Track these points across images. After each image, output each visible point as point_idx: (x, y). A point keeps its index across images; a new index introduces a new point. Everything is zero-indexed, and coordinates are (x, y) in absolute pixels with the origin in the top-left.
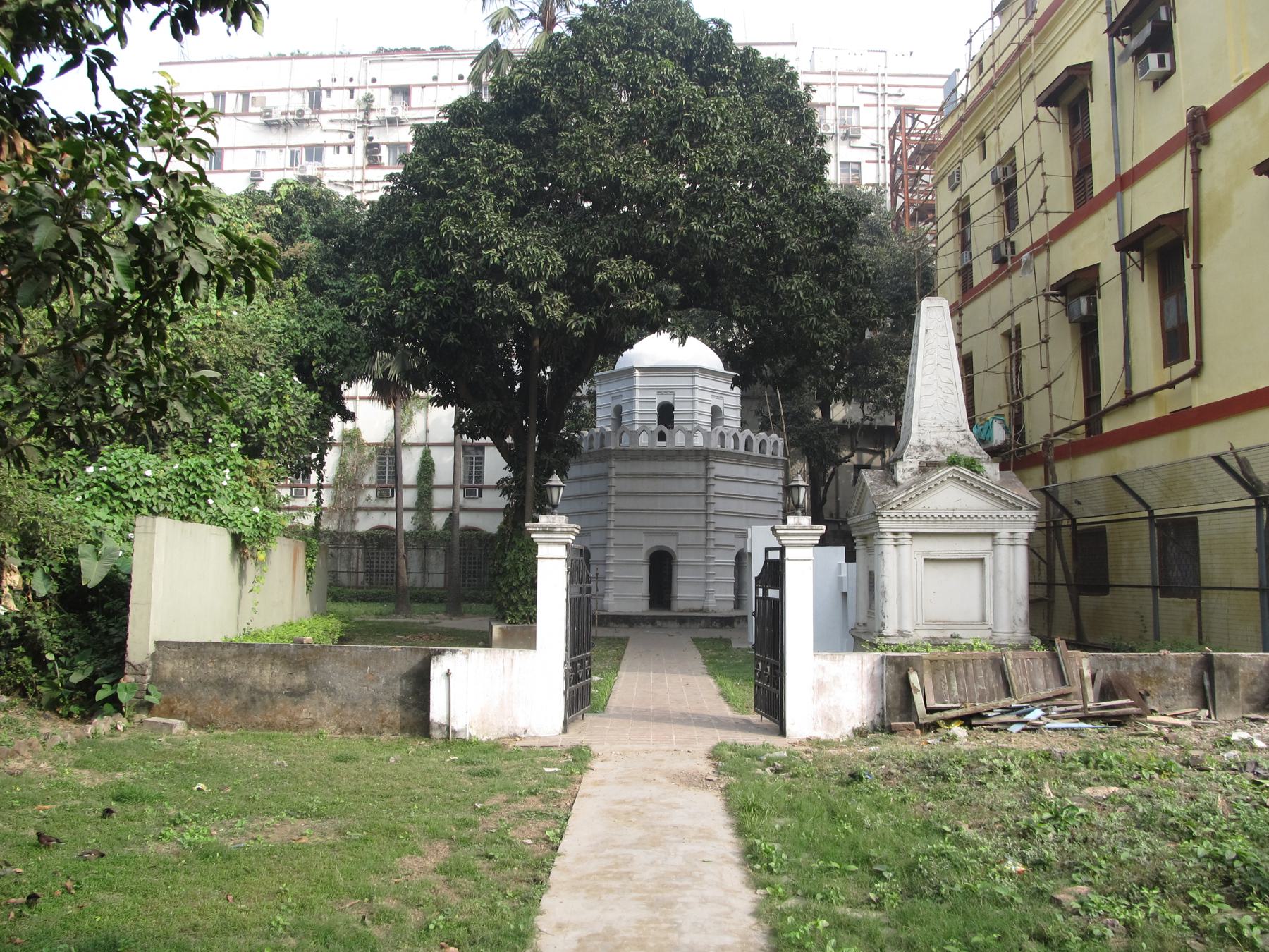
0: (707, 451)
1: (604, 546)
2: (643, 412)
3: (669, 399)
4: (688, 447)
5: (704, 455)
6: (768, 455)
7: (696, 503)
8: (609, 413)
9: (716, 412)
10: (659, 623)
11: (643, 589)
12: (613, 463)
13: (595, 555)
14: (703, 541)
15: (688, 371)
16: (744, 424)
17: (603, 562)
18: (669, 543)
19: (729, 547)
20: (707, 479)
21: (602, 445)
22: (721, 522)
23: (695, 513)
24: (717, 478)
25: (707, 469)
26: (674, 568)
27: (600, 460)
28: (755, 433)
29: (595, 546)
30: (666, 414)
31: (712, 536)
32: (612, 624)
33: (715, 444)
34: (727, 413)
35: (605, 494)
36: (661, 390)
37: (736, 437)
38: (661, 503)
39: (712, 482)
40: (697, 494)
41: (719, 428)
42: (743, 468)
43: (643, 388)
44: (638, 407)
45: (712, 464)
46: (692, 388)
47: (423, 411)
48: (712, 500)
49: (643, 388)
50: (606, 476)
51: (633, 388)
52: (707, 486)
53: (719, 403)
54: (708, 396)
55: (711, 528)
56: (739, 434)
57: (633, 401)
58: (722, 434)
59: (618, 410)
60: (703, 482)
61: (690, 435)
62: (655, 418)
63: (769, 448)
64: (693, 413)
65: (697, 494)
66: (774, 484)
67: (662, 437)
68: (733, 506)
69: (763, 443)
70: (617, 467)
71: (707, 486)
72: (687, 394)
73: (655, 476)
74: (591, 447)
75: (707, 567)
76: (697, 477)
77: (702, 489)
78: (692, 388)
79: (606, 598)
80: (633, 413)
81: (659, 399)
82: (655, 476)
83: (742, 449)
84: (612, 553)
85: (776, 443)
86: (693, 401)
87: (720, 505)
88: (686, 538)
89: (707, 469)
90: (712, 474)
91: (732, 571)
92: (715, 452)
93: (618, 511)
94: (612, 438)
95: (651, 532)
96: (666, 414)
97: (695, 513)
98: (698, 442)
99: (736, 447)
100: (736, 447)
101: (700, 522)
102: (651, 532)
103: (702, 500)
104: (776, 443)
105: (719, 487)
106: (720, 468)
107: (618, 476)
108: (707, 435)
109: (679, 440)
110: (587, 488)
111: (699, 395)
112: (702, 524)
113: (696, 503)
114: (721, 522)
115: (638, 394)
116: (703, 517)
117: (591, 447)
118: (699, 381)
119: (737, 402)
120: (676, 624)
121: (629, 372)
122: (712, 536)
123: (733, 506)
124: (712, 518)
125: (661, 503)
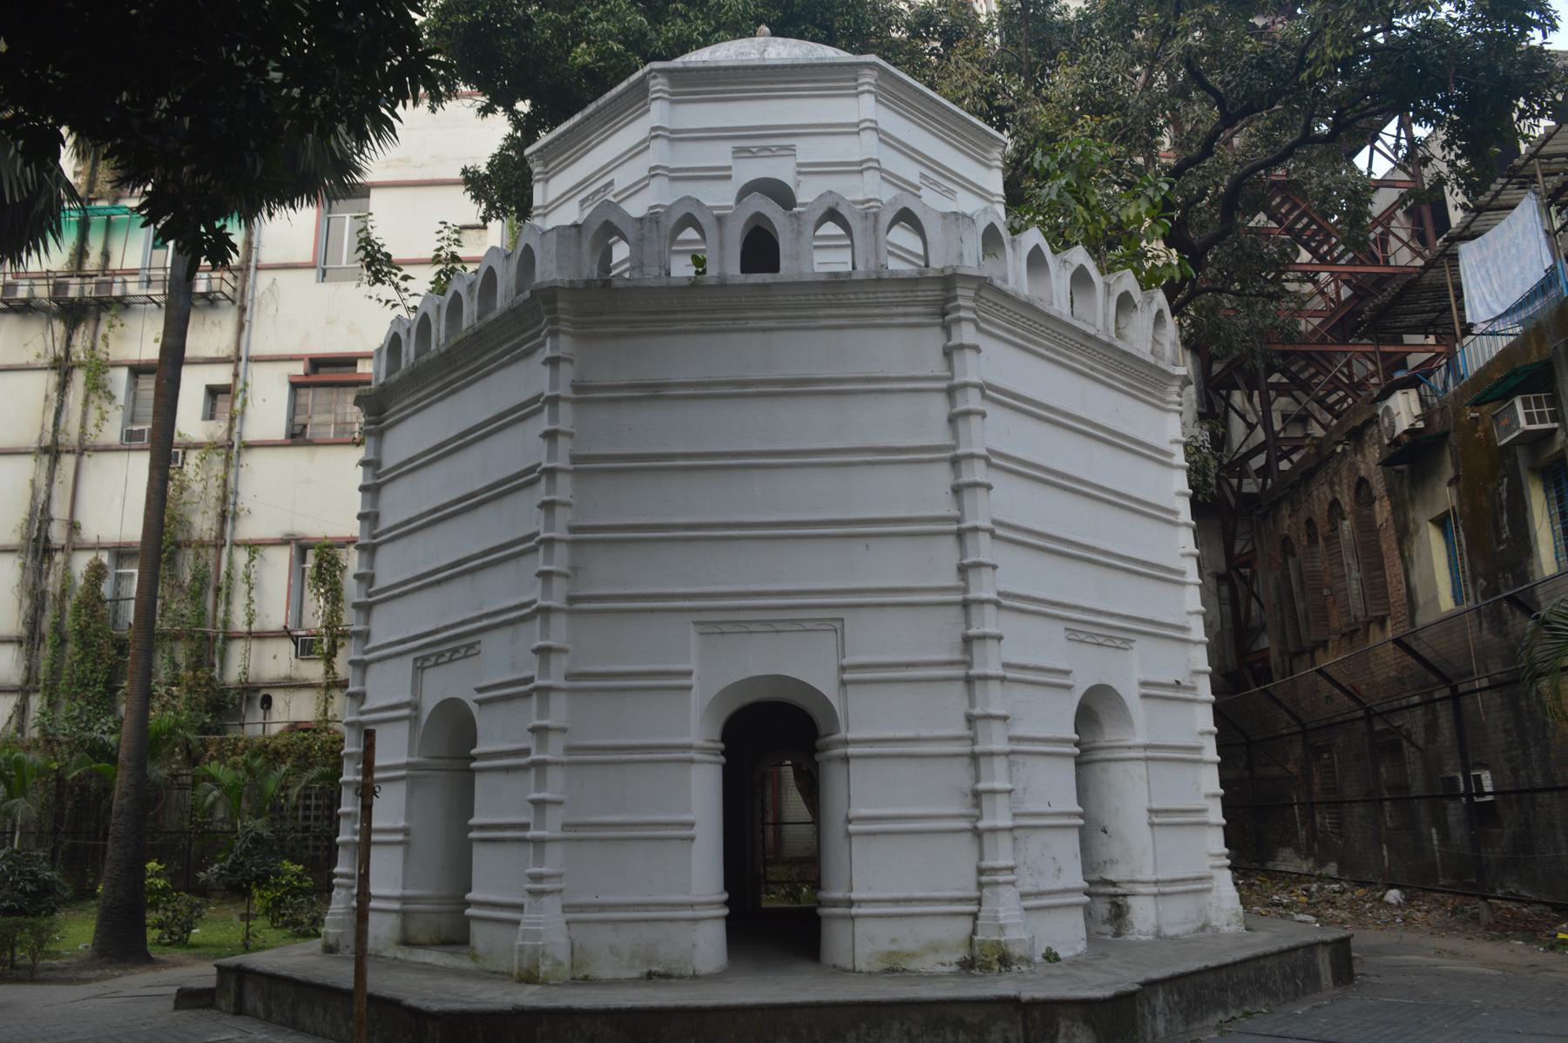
5: (938, 296)
11: (702, 873)
13: (496, 733)
18: (808, 664)
19: (1051, 679)
20: (951, 392)
22: (1016, 572)
29: (495, 697)
36: (748, 141)
39: (973, 401)
45: (966, 334)
54: (910, 171)
60: (938, 407)
67: (760, 248)
76: (911, 387)
77: (940, 436)
85: (1159, 316)
87: (1006, 500)
88: (876, 639)
90: (971, 369)
95: (721, 619)
102: (721, 619)
103: (942, 477)
105: (996, 431)
106: (996, 361)
114: (1016, 572)
116: (947, 553)
124: (983, 550)
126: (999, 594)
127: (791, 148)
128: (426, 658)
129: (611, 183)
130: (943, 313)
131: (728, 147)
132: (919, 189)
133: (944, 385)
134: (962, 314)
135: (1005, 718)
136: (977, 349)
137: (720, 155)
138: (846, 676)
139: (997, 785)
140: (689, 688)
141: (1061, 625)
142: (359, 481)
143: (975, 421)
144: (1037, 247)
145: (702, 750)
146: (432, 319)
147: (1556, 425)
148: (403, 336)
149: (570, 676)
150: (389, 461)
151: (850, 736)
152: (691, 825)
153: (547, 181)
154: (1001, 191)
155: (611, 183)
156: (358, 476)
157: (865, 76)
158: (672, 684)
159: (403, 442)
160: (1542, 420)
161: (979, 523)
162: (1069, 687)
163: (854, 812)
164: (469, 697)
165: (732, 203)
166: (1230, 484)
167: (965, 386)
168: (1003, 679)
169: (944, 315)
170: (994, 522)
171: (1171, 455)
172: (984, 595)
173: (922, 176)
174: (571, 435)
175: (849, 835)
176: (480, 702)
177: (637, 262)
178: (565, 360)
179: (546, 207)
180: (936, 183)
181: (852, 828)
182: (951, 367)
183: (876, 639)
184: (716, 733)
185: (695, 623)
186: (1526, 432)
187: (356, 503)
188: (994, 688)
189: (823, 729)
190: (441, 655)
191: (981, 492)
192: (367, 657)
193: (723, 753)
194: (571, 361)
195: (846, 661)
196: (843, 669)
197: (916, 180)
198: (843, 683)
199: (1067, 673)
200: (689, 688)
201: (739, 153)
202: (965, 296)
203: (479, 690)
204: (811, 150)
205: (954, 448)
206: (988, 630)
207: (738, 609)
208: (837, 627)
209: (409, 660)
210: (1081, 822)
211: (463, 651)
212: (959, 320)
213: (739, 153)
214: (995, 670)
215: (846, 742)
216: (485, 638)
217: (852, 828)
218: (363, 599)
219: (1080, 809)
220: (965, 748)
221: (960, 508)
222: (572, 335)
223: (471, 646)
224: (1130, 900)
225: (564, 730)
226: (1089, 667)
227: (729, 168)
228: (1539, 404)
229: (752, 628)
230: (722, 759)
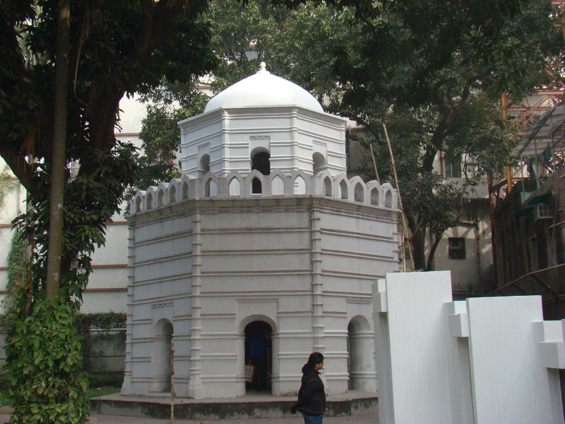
0: (311, 199)
1: (189, 318)
2: (235, 159)
3: (263, 144)
4: (288, 195)
5: (307, 205)
6: (381, 206)
7: (298, 262)
8: (196, 164)
9: (318, 161)
10: (257, 412)
12: (198, 217)
13: (178, 329)
14: (308, 308)
15: (285, 111)
16: (351, 172)
17: (188, 338)
18: (268, 312)
19: (340, 315)
20: (312, 233)
21: (185, 197)
22: (329, 285)
23: (299, 273)
24: (323, 231)
25: (311, 220)
26: (275, 342)
27: (182, 215)
28: (366, 181)
30: (261, 160)
31: (319, 301)
32: (198, 415)
33: (319, 191)
34: (331, 161)
35: (189, 255)
36: (255, 135)
37: (343, 184)
38: (257, 263)
40: (300, 251)
41: (324, 174)
42: (353, 221)
43: (233, 133)
44: (228, 154)
45: (317, 215)
46: (291, 131)
47: (15, 192)
48: (318, 257)
49: (233, 133)
50: (190, 233)
51: (222, 133)
52: (312, 241)
53: (322, 150)
54: (308, 141)
55: (318, 291)
56: (348, 182)
57: (222, 147)
58: (327, 181)
59: (206, 162)
60: (306, 236)
61: (289, 179)
62: (248, 166)
63: (382, 198)
64: (292, 159)
65: (300, 251)
66: (388, 240)
67: (257, 186)
68: (343, 265)
69: (375, 191)
70: (203, 221)
71: (312, 241)
72: (285, 138)
73: (249, 231)
74: (173, 200)
75: (315, 339)
76: (299, 230)
78: (291, 131)
79: (191, 382)
80: (222, 161)
81: (253, 145)
82: (249, 231)
83: (351, 199)
84: (198, 326)
85: (389, 193)
86: (292, 145)
87: (328, 263)
88: (289, 304)
89: (311, 220)
90: (318, 226)
91: (344, 344)
92: (320, 200)
93: (205, 275)
94: (197, 185)
95: (244, 298)
96: (261, 160)
97: (299, 273)
98: (300, 189)
99: (344, 196)
100: (344, 196)
101: (305, 284)
102: (244, 298)
103: (307, 257)
104: (389, 193)
106: (326, 220)
107: (204, 232)
108: (310, 180)
109: (275, 188)
110: (169, 248)
111: (299, 139)
112: (308, 287)
113: (298, 262)
114: (329, 285)
115: (228, 140)
116: (308, 280)
117: (173, 200)
118: (299, 123)
119: (341, 150)
120: (278, 413)
121: (218, 114)
122: (319, 301)
123: (343, 265)
125: (257, 263)
126: (323, 292)
127: (269, 137)
128: (155, 305)
129: (209, 143)
130: (310, 210)
131: (248, 136)
132: (312, 147)
133: (309, 230)
134: (315, 209)
135: (323, 328)
136: (319, 219)
137: (245, 140)
138: (279, 315)
139: (319, 346)
140: (235, 318)
141: (344, 299)
142: (128, 246)
143: (317, 242)
144: (343, 180)
145: (238, 335)
146: (153, 195)
147: (551, 217)
148: (142, 198)
149: (201, 315)
150: (138, 239)
151: (280, 332)
152: (236, 356)
153: (185, 134)
154: (344, 139)
155: (209, 143)
156: (127, 243)
157: (293, 111)
158: (231, 316)
159: (144, 233)
160: (546, 215)
161: (317, 272)
162: (346, 317)
163: (280, 353)
164: (170, 318)
165: (249, 156)
166: (495, 195)
167: (315, 231)
168: (323, 317)
169: (310, 208)
170: (322, 271)
171: (392, 239)
172: (318, 293)
173: (314, 141)
174: (201, 245)
175: (279, 359)
176: (174, 321)
177: (219, 192)
178: (198, 222)
179: (186, 144)
180: (319, 142)
181: (280, 357)
182: (311, 225)
183: (289, 304)
184: (243, 330)
185: (237, 300)
186: (539, 220)
187: (127, 253)
188: (320, 320)
189: (273, 329)
190: (161, 305)
191: (318, 264)
192: (134, 303)
193: (245, 336)
194: (200, 222)
195: (279, 311)
196: (279, 313)
197: (312, 145)
198: (278, 317)
199: (345, 313)
200: (235, 318)
201: (252, 138)
202: (315, 203)
203: (174, 317)
204: (275, 138)
205: (312, 250)
206: (319, 303)
207: (249, 296)
208: (277, 301)
209: (150, 304)
210: (348, 356)
211: (168, 305)
212: (314, 211)
213: (251, 137)
214: (320, 314)
215: (279, 334)
216: (175, 301)
217: (280, 357)
218: (131, 285)
219: (347, 352)
220: (312, 336)
221: (312, 268)
222: (200, 214)
223: (171, 303)
224: (368, 380)
225: (200, 330)
226: (353, 311)
227: (248, 144)
228: (545, 209)
229: (253, 301)
230: (244, 338)
